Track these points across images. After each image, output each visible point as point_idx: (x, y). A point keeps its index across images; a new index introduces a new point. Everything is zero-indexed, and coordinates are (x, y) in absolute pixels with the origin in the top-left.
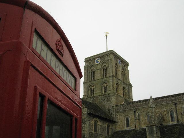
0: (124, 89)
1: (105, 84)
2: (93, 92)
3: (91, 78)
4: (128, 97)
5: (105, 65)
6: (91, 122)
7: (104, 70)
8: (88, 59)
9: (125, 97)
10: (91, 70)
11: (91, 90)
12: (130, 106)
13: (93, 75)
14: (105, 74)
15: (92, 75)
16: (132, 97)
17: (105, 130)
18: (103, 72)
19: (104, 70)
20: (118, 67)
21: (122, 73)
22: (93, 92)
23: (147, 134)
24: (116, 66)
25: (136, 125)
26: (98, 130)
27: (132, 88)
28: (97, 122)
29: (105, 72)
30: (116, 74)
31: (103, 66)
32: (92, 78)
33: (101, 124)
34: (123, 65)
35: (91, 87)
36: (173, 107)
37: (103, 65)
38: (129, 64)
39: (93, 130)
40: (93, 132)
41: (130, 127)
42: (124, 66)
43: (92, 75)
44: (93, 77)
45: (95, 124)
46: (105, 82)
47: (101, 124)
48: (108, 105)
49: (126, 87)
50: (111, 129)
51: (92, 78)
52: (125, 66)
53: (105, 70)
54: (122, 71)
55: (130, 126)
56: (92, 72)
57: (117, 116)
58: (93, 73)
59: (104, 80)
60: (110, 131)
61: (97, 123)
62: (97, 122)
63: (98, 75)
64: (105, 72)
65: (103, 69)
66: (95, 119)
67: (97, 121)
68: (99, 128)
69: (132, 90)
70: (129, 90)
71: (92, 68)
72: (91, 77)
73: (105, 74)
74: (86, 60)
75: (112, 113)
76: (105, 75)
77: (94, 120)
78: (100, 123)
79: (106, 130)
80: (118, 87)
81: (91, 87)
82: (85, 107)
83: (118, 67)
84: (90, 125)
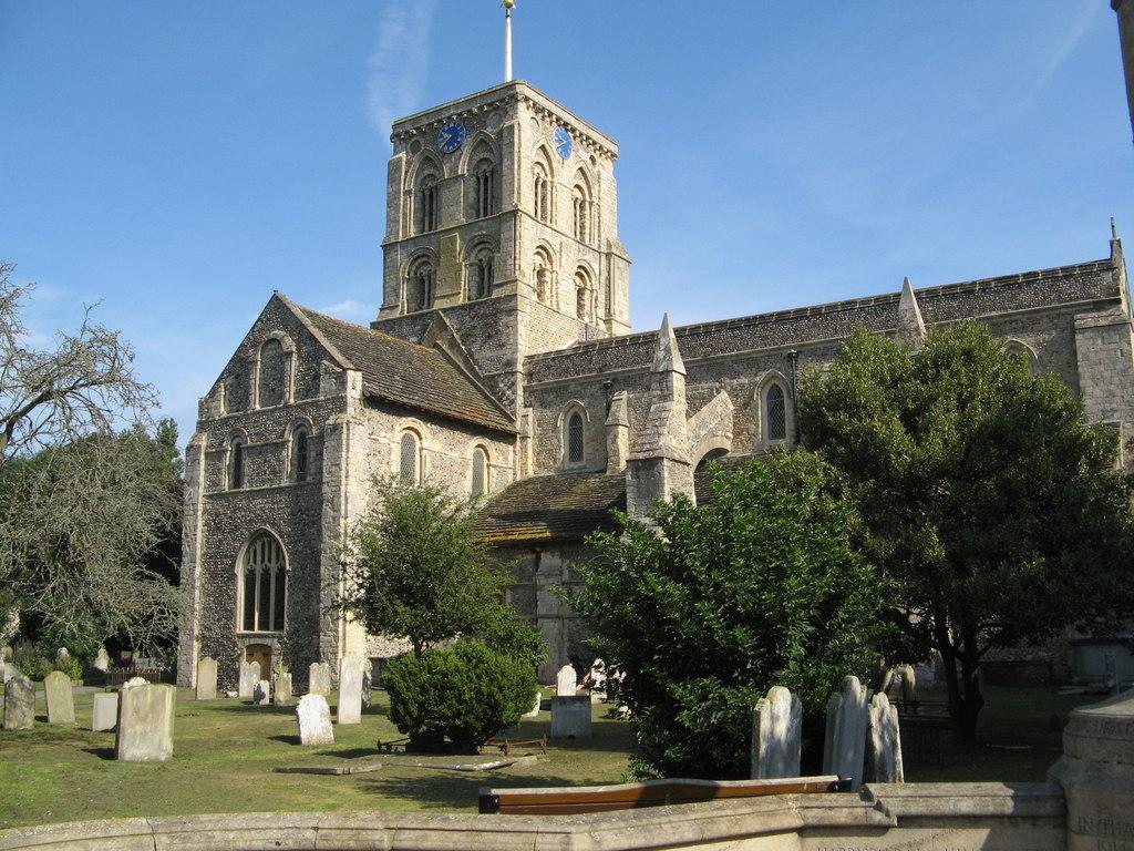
0: (582, 272)
1: (484, 253)
2: (426, 290)
4: (601, 312)
5: (486, 155)
6: (381, 440)
7: (482, 181)
12: (590, 362)
13: (431, 205)
14: (486, 199)
20: (554, 164)
21: (577, 193)
22: (426, 290)
29: (486, 189)
30: (544, 199)
32: (427, 218)
35: (418, 268)
37: (477, 158)
41: (584, 463)
42: (592, 158)
43: (427, 207)
44: (431, 214)
45: (407, 444)
46: (480, 243)
47: (437, 447)
48: (489, 354)
49: (596, 267)
51: (427, 218)
52: (598, 160)
53: (486, 179)
54: (577, 186)
55: (585, 455)
56: (427, 193)
58: (431, 196)
62: (416, 437)
64: (486, 189)
65: (478, 179)
67: (418, 433)
71: (426, 172)
73: (486, 199)
75: (504, 394)
76: (485, 208)
77: (398, 428)
79: (469, 473)
80: (548, 267)
82: (351, 366)
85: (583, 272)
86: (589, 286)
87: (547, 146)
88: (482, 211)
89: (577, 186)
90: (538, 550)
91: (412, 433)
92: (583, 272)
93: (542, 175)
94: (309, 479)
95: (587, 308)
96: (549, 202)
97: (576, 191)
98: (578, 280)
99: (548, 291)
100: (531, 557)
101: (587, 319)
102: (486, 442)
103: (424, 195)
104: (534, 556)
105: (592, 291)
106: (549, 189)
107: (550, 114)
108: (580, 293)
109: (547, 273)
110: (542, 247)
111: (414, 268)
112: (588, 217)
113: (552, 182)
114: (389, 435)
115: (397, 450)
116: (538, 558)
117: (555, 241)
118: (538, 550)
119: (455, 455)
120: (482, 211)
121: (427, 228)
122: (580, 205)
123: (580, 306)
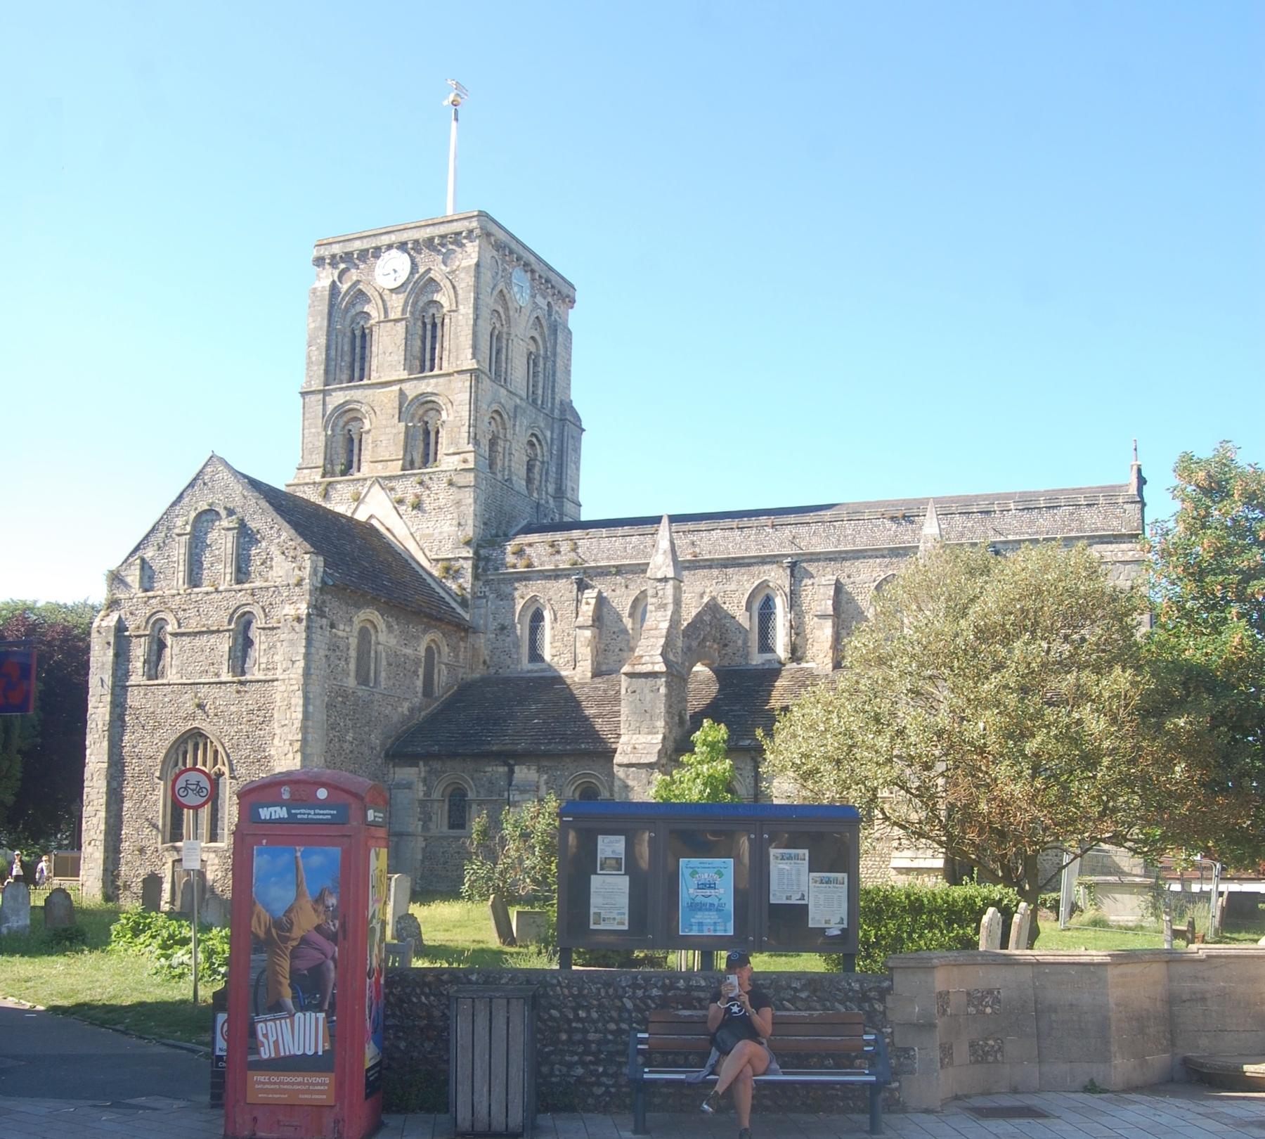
4: (551, 488)
7: (429, 327)
8: (337, 249)
9: (539, 490)
10: (352, 322)
15: (358, 350)
16: (575, 490)
17: (415, 672)
18: (424, 343)
19: (429, 327)
20: (511, 313)
23: (624, 709)
24: (501, 310)
25: (580, 657)
27: (578, 440)
28: (372, 631)
31: (421, 304)
32: (357, 365)
33: (393, 642)
36: (778, 577)
39: (352, 674)
40: (351, 682)
43: (358, 350)
49: (548, 434)
50: (446, 664)
51: (357, 365)
54: (533, 338)
56: (358, 333)
57: (485, 597)
61: (373, 638)
62: (372, 631)
65: (424, 324)
67: (375, 627)
68: (384, 663)
69: (577, 450)
70: (561, 451)
72: (347, 358)
74: (326, 252)
76: (433, 360)
79: (421, 671)
81: (345, 419)
83: (508, 317)
84: (333, 647)
85: (534, 440)
86: (539, 458)
87: (505, 291)
88: (428, 364)
89: (533, 338)
90: (512, 762)
91: (369, 626)
92: (534, 440)
93: (498, 325)
95: (537, 483)
96: (503, 357)
97: (531, 342)
99: (499, 463)
100: (503, 769)
101: (535, 495)
103: (354, 334)
104: (506, 769)
105: (543, 463)
106: (504, 342)
107: (511, 252)
108: (530, 469)
109: (501, 443)
110: (496, 411)
111: (341, 423)
112: (541, 375)
113: (509, 334)
114: (348, 629)
115: (353, 642)
116: (512, 772)
118: (512, 762)
119: (408, 651)
120: (428, 364)
121: (357, 375)
122: (532, 359)
123: (529, 481)
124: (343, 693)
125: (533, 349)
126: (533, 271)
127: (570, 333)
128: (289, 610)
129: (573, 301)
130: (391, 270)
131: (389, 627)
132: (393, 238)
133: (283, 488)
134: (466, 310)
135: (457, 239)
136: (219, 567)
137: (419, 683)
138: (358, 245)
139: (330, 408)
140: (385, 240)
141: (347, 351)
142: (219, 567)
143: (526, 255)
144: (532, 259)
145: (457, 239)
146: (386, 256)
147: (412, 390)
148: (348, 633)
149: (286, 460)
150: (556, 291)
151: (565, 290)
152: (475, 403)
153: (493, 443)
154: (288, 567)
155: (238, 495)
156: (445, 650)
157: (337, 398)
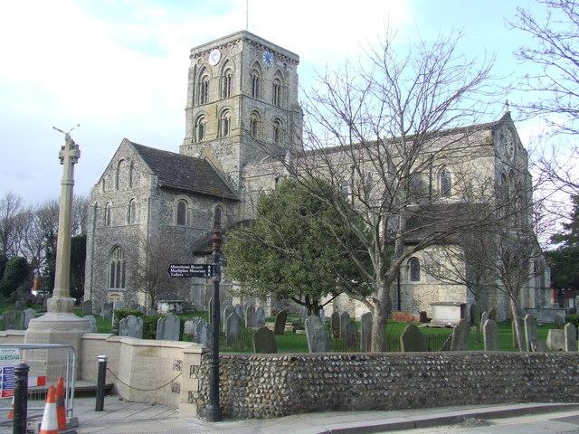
3: (203, 97)
8: (197, 51)
11: (201, 127)
18: (226, 84)
21: (276, 82)
26: (188, 221)
30: (257, 87)
33: (196, 207)
34: (280, 64)
38: (300, 60)
40: (174, 224)
45: (181, 208)
47: (196, 207)
59: (224, 103)
60: (224, 219)
63: (214, 93)
66: (180, 197)
68: (191, 216)
78: (192, 205)
84: (163, 211)
94: (136, 223)
98: (275, 125)
102: (222, 204)
107: (261, 46)
117: (261, 107)
119: (205, 211)
123: (277, 138)
124: (170, 229)
125: (276, 82)
126: (274, 52)
127: (297, 75)
128: (144, 197)
129: (297, 62)
130: (214, 58)
131: (195, 202)
132: (215, 45)
133: (177, 151)
134: (238, 71)
135: (234, 43)
136: (125, 182)
137: (212, 224)
138: (204, 49)
139: (194, 115)
140: (212, 46)
141: (200, 90)
142: (125, 182)
143: (268, 46)
144: (273, 48)
145: (234, 43)
146: (212, 53)
147: (220, 105)
148: (173, 204)
149: (171, 136)
150: (288, 60)
151: (292, 57)
152: (241, 108)
153: (254, 123)
154: (146, 181)
155: (132, 151)
156: (225, 209)
157: (196, 110)
